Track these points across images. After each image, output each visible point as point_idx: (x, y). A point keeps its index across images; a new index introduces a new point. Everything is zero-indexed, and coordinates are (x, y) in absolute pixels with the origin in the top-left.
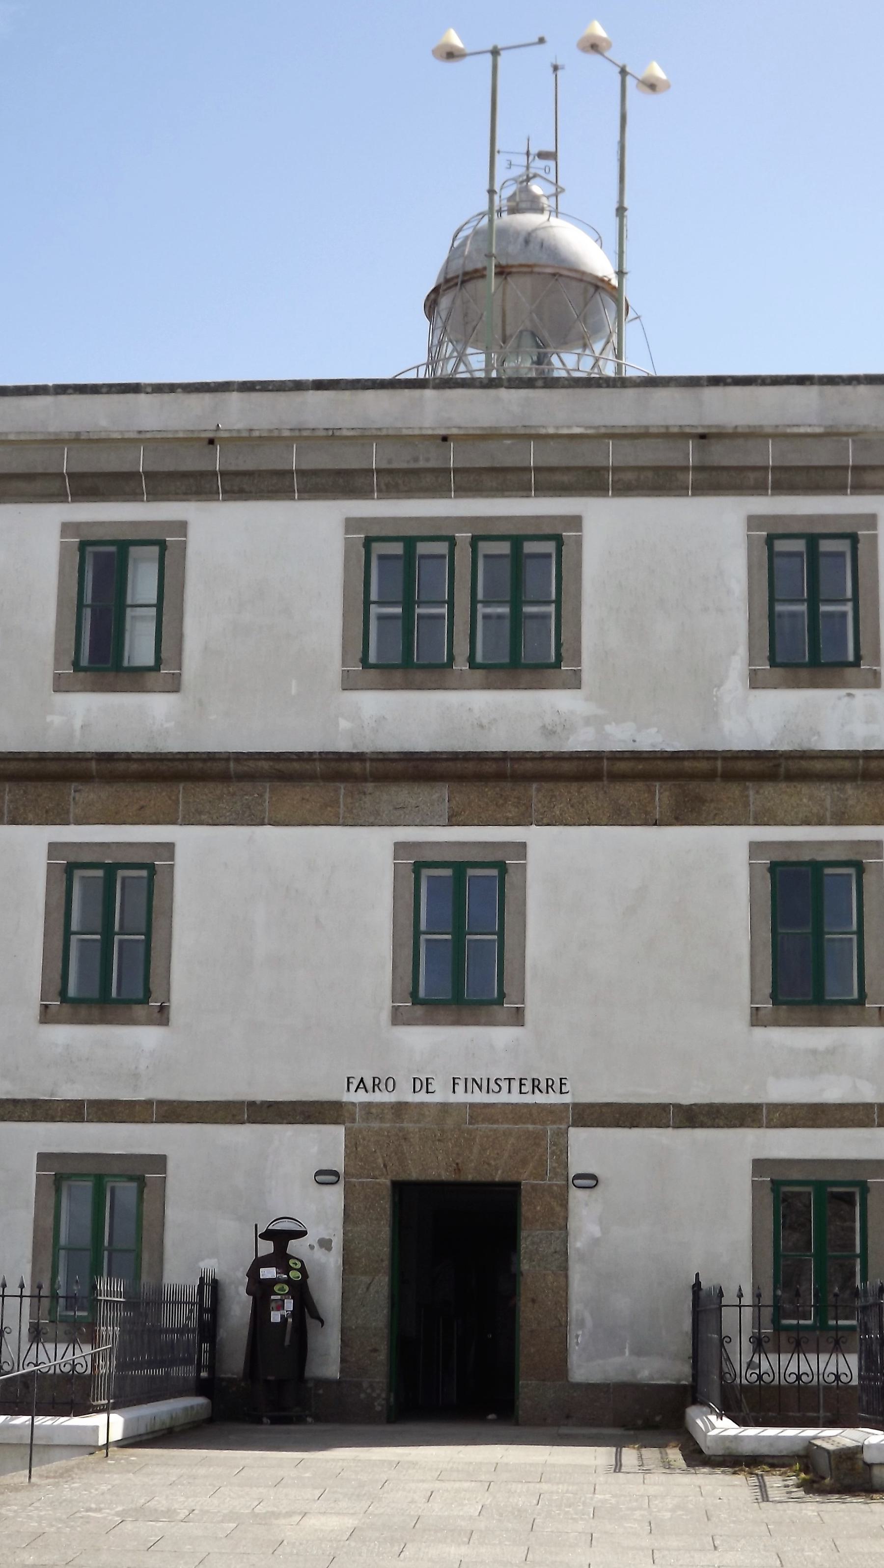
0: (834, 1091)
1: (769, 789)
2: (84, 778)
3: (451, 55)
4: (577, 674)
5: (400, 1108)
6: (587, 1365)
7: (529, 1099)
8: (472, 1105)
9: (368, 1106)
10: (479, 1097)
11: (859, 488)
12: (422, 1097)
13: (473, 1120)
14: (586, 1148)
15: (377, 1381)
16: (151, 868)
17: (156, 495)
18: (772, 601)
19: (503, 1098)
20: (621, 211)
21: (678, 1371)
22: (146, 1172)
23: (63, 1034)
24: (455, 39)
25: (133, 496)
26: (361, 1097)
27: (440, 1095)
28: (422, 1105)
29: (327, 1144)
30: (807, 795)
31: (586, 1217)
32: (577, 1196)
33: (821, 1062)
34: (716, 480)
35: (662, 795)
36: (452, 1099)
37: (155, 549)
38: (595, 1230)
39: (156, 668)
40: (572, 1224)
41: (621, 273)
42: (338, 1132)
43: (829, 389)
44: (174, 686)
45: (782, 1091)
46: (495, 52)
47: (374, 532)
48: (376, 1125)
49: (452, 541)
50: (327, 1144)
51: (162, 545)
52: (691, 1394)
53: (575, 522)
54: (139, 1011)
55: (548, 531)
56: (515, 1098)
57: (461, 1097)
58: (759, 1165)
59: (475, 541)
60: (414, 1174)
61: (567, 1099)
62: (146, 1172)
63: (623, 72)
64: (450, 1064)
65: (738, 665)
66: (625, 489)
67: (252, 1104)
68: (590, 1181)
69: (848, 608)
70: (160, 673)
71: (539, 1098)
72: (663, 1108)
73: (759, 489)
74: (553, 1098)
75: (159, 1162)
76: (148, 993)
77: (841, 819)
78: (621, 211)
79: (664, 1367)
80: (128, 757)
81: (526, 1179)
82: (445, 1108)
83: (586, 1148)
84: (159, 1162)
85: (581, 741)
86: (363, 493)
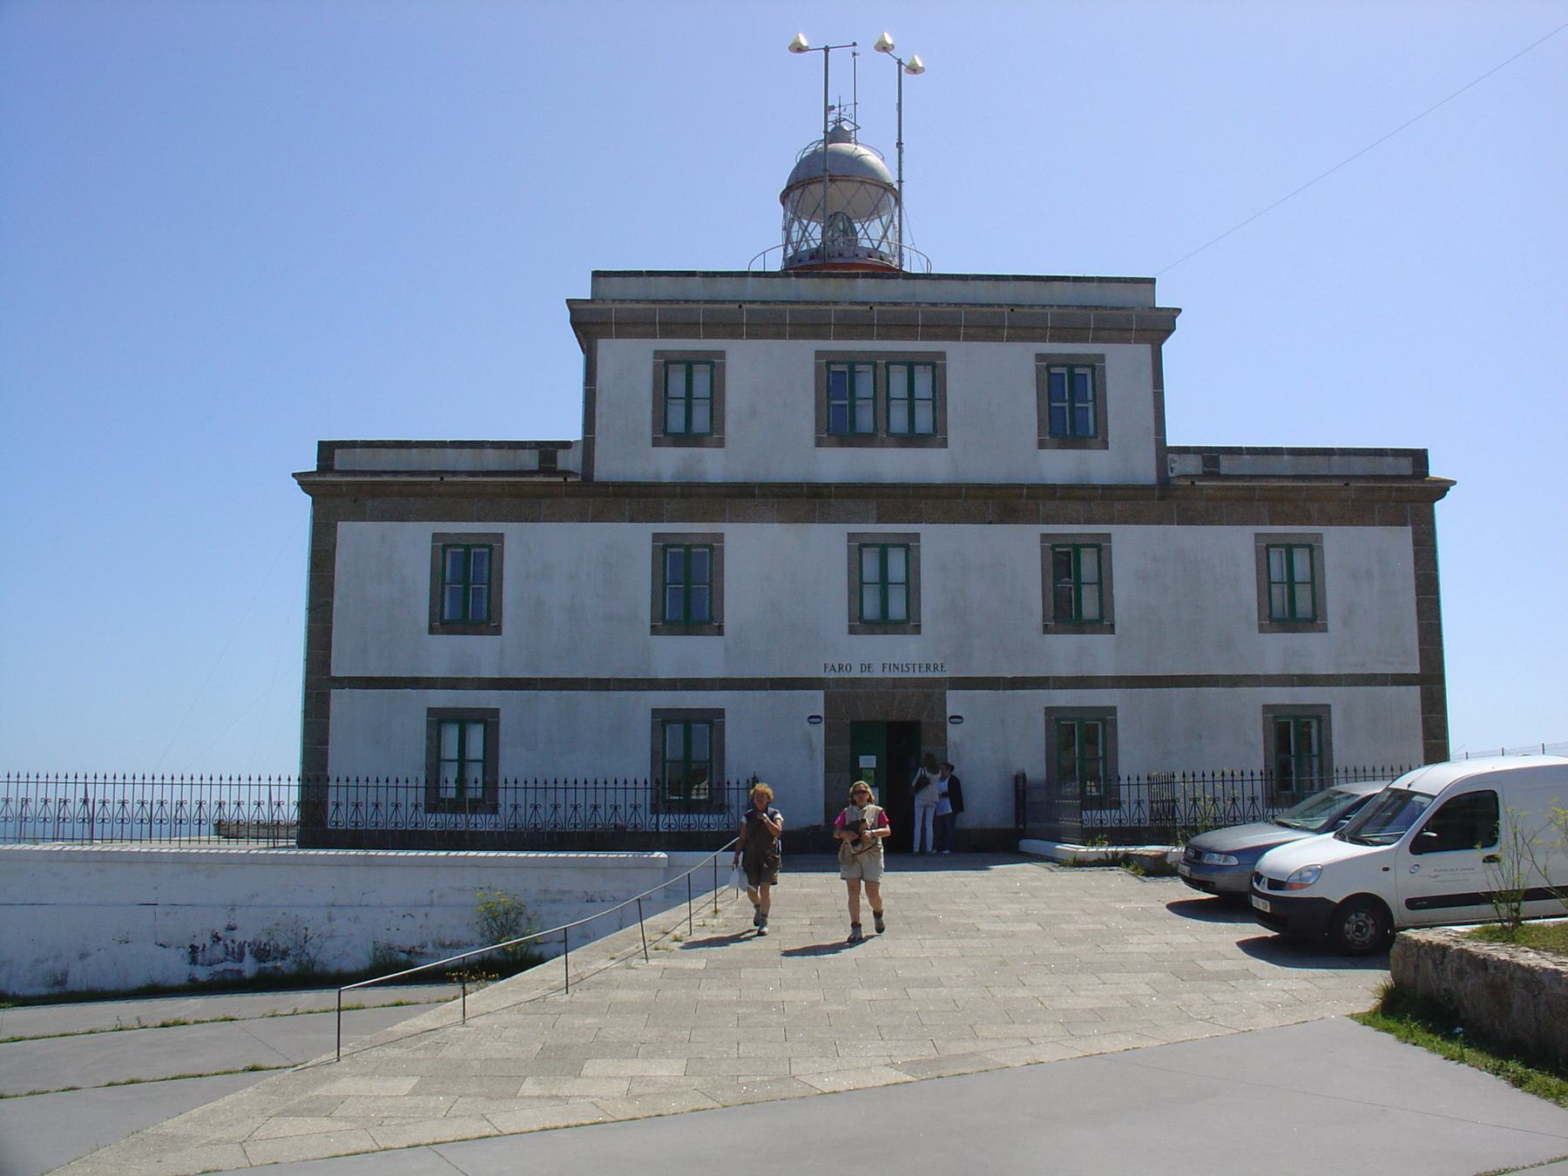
2: (674, 496)
3: (799, 49)
5: (854, 681)
7: (925, 675)
11: (1096, 340)
12: (866, 675)
13: (895, 686)
16: (712, 548)
17: (708, 336)
18: (1050, 400)
19: (910, 675)
20: (899, 144)
22: (714, 718)
24: (804, 42)
25: (696, 336)
26: (832, 675)
27: (877, 673)
29: (815, 702)
37: (707, 367)
39: (711, 434)
41: (900, 181)
42: (821, 694)
44: (721, 443)
46: (827, 49)
49: (875, 366)
51: (712, 365)
52: (1022, 834)
56: (918, 675)
58: (1049, 711)
59: (887, 365)
62: (714, 718)
63: (900, 62)
67: (771, 680)
68: (957, 719)
69: (1090, 405)
70: (714, 436)
71: (930, 675)
73: (1042, 339)
74: (937, 675)
75: (720, 713)
76: (712, 618)
78: (899, 144)
81: (923, 719)
83: (955, 702)
84: (720, 713)
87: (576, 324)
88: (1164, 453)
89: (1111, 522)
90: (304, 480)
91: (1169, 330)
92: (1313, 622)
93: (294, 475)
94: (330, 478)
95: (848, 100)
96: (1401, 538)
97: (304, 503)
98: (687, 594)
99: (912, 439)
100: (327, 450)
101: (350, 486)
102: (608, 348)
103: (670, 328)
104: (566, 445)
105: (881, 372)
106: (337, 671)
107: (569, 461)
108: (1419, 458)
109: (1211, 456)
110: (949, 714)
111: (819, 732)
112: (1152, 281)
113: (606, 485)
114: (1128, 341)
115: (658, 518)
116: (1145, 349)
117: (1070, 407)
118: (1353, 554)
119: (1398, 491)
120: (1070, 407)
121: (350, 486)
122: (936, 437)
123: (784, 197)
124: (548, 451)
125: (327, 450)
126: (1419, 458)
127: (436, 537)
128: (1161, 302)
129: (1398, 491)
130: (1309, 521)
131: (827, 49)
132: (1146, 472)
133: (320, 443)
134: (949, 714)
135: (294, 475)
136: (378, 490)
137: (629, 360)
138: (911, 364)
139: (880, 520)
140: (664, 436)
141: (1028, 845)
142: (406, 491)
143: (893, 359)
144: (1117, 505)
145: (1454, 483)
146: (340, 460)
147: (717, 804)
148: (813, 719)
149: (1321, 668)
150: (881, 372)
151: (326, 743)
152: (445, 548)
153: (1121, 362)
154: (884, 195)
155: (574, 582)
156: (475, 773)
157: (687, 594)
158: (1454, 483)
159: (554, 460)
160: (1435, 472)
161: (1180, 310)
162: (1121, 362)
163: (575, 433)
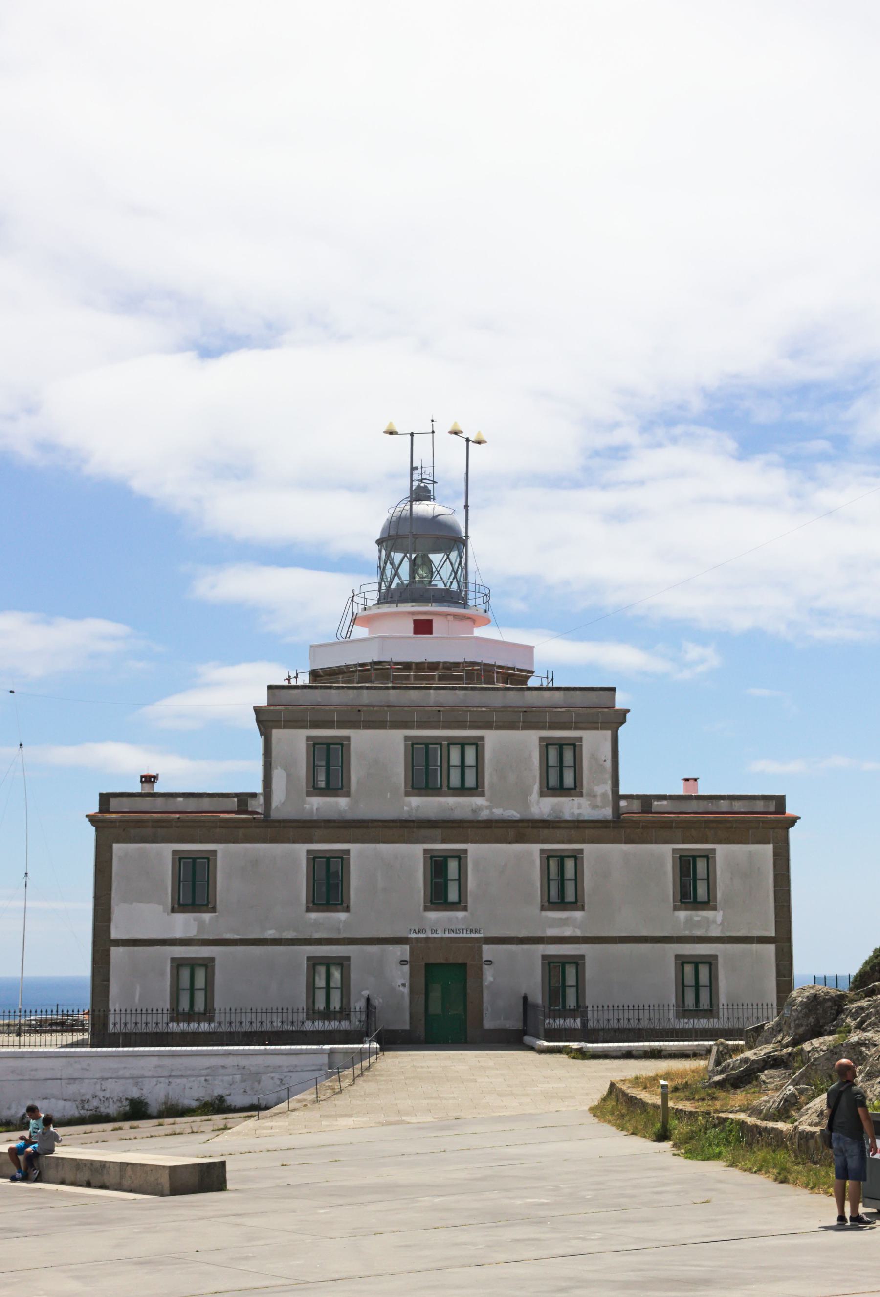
0: (568, 932)
1: (546, 831)
4: (483, 792)
5: (427, 939)
6: (489, 1024)
8: (451, 938)
9: (416, 938)
10: (453, 935)
11: (576, 728)
12: (435, 935)
14: (488, 951)
15: (421, 1031)
19: (461, 935)
20: (466, 507)
21: (519, 1025)
23: (313, 915)
26: (414, 935)
27: (440, 934)
28: (434, 938)
29: (404, 951)
30: (559, 833)
31: (489, 975)
32: (485, 967)
33: (564, 922)
34: (529, 726)
35: (512, 833)
36: (444, 936)
38: (491, 979)
40: (484, 977)
42: (407, 947)
43: (567, 692)
45: (551, 932)
46: (412, 434)
47: (415, 742)
48: (419, 945)
49: (441, 745)
50: (404, 951)
52: (524, 1032)
53: (482, 738)
54: (339, 907)
55: (473, 742)
56: (465, 935)
57: (447, 935)
58: (544, 957)
59: (449, 745)
60: (432, 961)
61: (482, 935)
63: (468, 440)
64: (441, 923)
65: (536, 788)
66: (498, 728)
68: (489, 962)
71: (473, 935)
72: (513, 938)
73: (543, 728)
74: (477, 935)
77: (570, 842)
78: (466, 507)
79: (514, 1023)
80: (334, 821)
82: (442, 938)
83: (488, 951)
85: (484, 815)
86: (411, 728)
87: (259, 721)
88: (617, 796)
89: (583, 842)
90: (92, 819)
91: (623, 721)
92: (708, 904)
93: (87, 816)
94: (108, 816)
95: (427, 463)
96: (768, 849)
97: (90, 831)
98: (328, 886)
99: (462, 790)
100: (105, 799)
101: (121, 821)
102: (277, 734)
103: (316, 725)
104: (254, 795)
105: (445, 749)
106: (115, 934)
107: (257, 805)
108: (780, 801)
109: (646, 801)
110: (484, 959)
111: (406, 968)
112: (613, 689)
113: (279, 821)
114: (597, 729)
115: (311, 841)
116: (608, 733)
117: (561, 772)
118: (734, 861)
119: (766, 822)
120: (561, 772)
121: (121, 821)
122: (477, 790)
123: (379, 542)
124: (243, 799)
125: (105, 799)
126: (780, 801)
127: (175, 852)
128: (619, 705)
129: (766, 822)
130: (707, 842)
131: (412, 434)
132: (607, 813)
133: (101, 795)
134: (485, 958)
135: (87, 816)
136: (139, 824)
137: (294, 742)
138: (463, 744)
139: (444, 841)
140: (314, 790)
141: (527, 1039)
142: (159, 824)
143: (452, 742)
144: (587, 832)
145: (799, 818)
146: (114, 803)
147: (344, 1013)
148: (403, 962)
149: (715, 932)
150: (445, 749)
151: (108, 980)
152: (180, 859)
153: (594, 741)
154: (452, 540)
155: (263, 880)
156: (200, 998)
157: (328, 886)
158: (799, 818)
159: (247, 805)
160: (791, 810)
161: (628, 711)
162: (594, 741)
163: (258, 788)
